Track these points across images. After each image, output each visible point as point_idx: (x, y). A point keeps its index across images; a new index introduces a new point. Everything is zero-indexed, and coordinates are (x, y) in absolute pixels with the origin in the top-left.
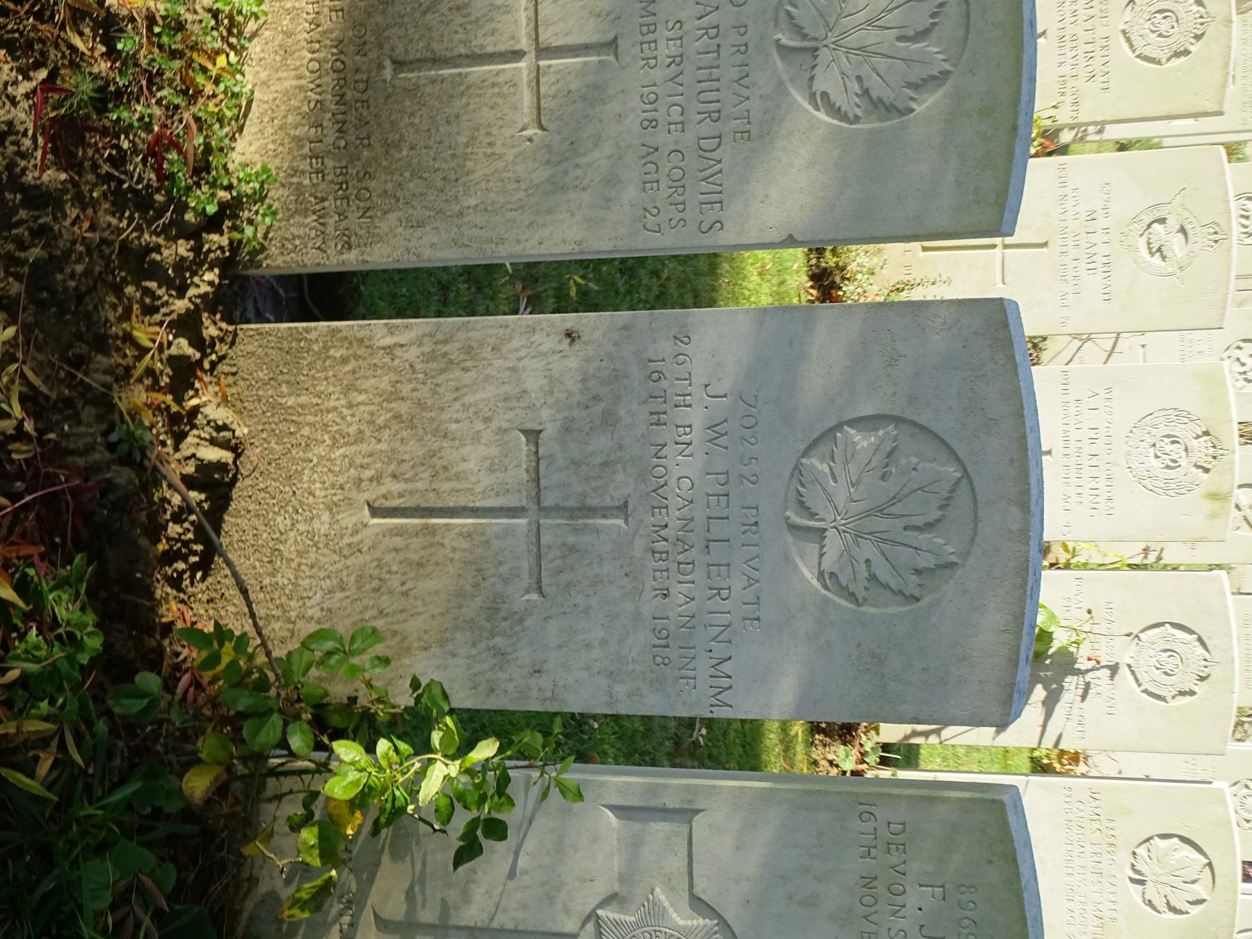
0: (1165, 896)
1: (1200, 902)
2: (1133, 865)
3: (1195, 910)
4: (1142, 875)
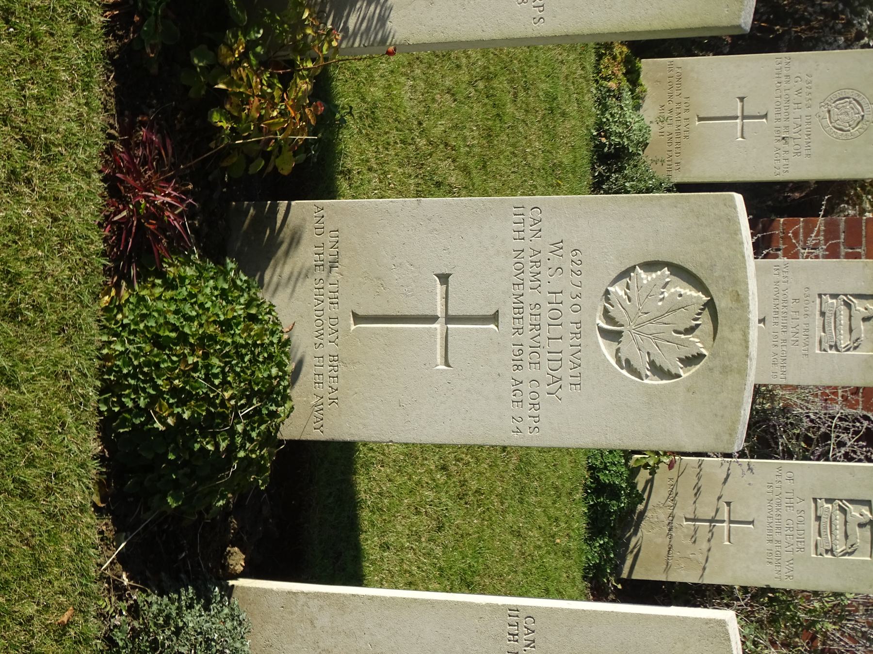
0: (648, 353)
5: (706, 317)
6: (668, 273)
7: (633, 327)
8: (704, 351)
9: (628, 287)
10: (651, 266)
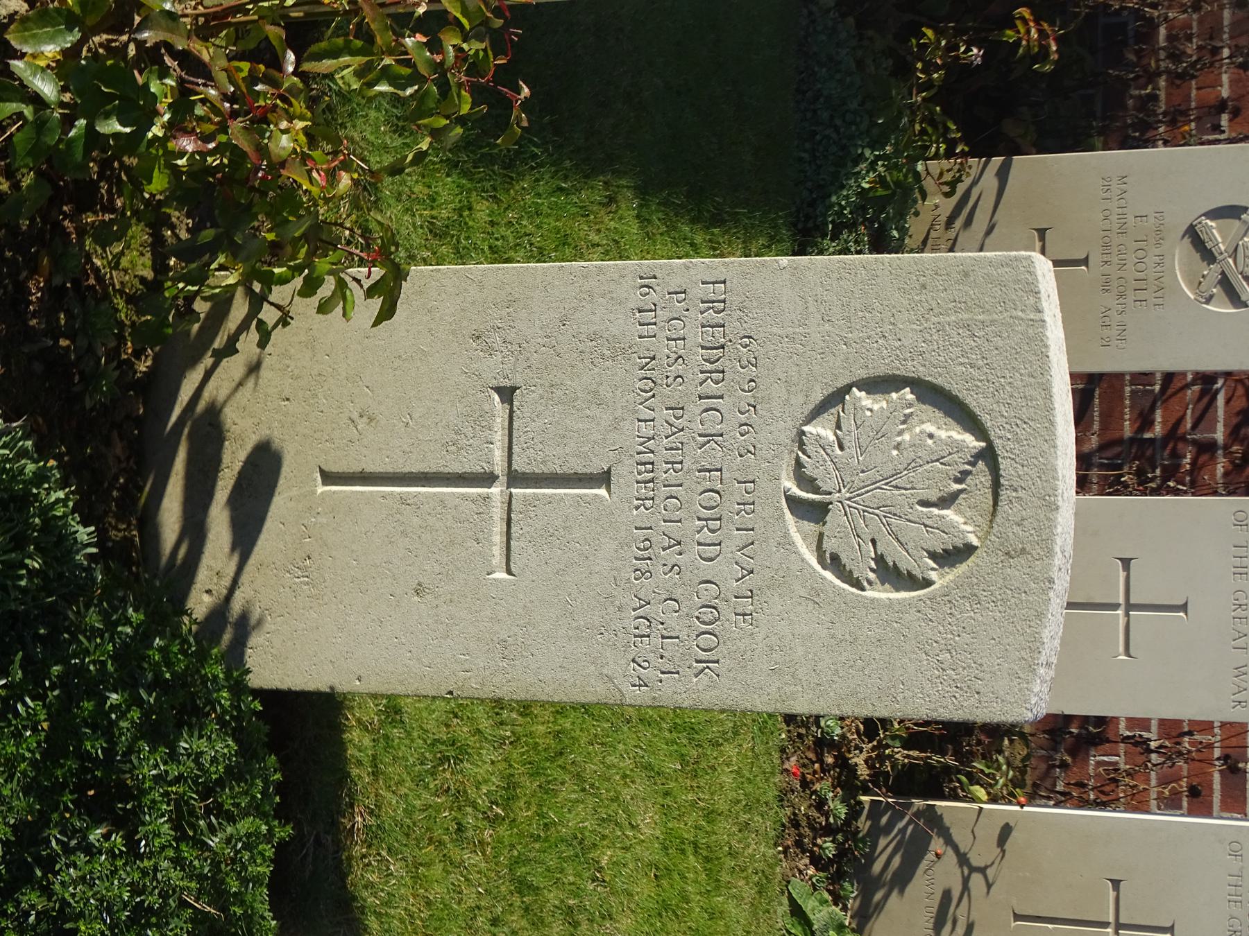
0: (874, 542)
1: (960, 553)
2: (799, 464)
3: (941, 579)
4: (817, 490)
5: (981, 476)
6: (911, 397)
7: (848, 495)
8: (974, 541)
9: (838, 427)
10: (879, 385)
